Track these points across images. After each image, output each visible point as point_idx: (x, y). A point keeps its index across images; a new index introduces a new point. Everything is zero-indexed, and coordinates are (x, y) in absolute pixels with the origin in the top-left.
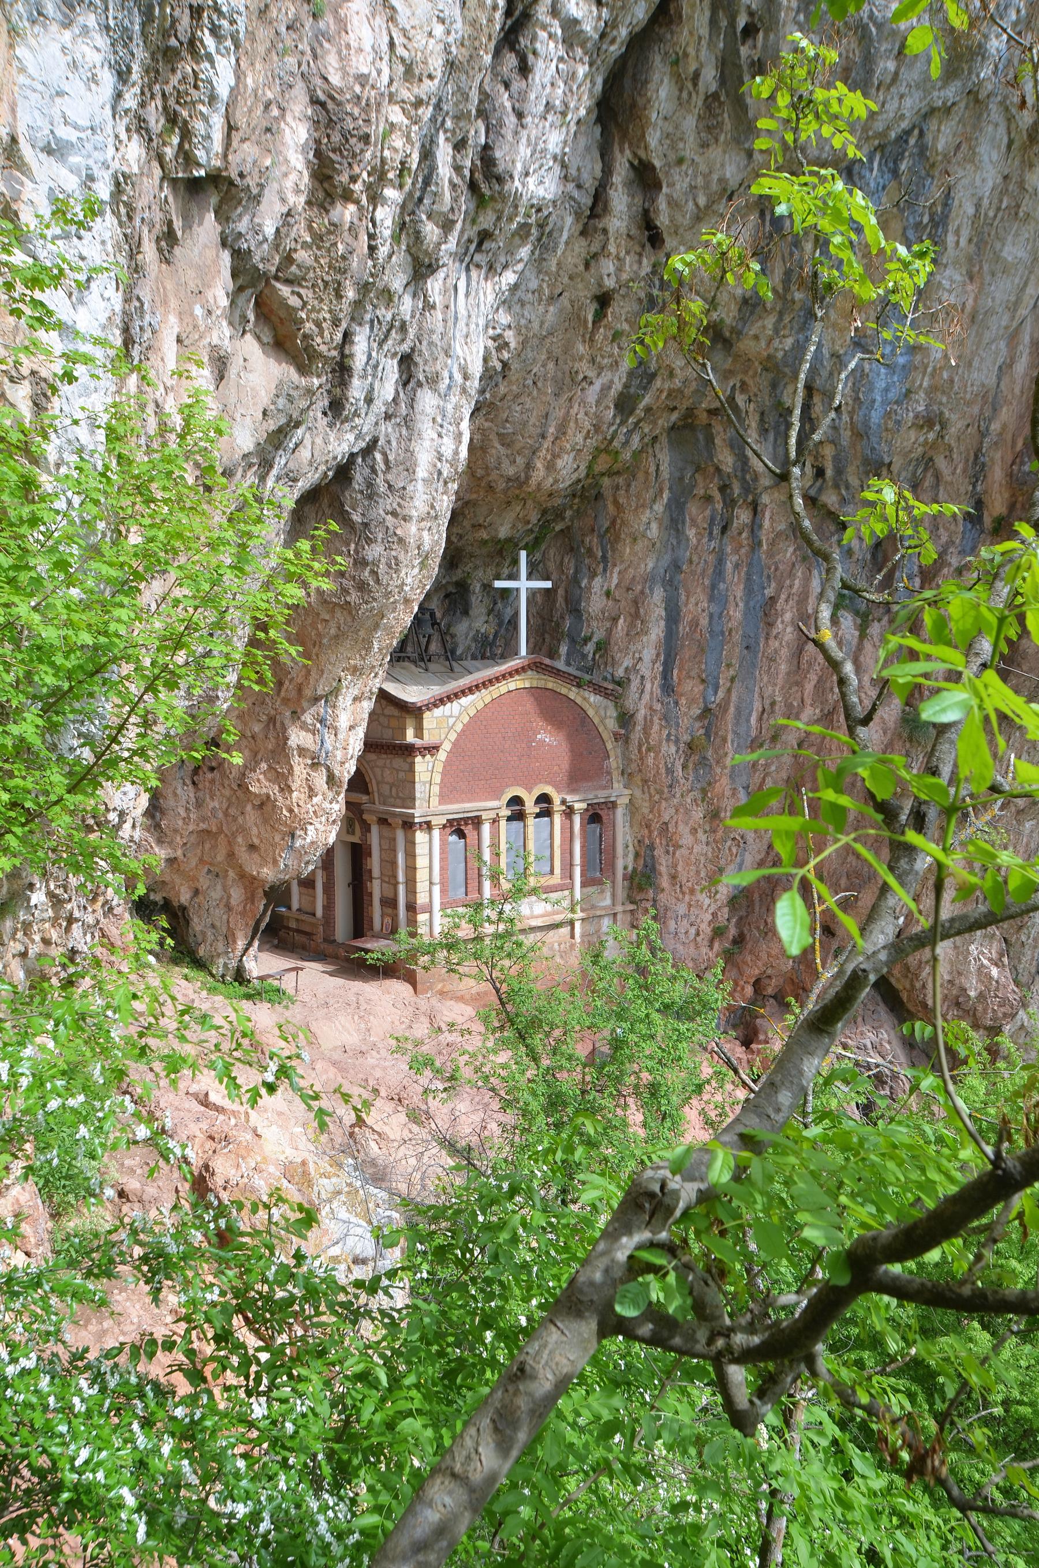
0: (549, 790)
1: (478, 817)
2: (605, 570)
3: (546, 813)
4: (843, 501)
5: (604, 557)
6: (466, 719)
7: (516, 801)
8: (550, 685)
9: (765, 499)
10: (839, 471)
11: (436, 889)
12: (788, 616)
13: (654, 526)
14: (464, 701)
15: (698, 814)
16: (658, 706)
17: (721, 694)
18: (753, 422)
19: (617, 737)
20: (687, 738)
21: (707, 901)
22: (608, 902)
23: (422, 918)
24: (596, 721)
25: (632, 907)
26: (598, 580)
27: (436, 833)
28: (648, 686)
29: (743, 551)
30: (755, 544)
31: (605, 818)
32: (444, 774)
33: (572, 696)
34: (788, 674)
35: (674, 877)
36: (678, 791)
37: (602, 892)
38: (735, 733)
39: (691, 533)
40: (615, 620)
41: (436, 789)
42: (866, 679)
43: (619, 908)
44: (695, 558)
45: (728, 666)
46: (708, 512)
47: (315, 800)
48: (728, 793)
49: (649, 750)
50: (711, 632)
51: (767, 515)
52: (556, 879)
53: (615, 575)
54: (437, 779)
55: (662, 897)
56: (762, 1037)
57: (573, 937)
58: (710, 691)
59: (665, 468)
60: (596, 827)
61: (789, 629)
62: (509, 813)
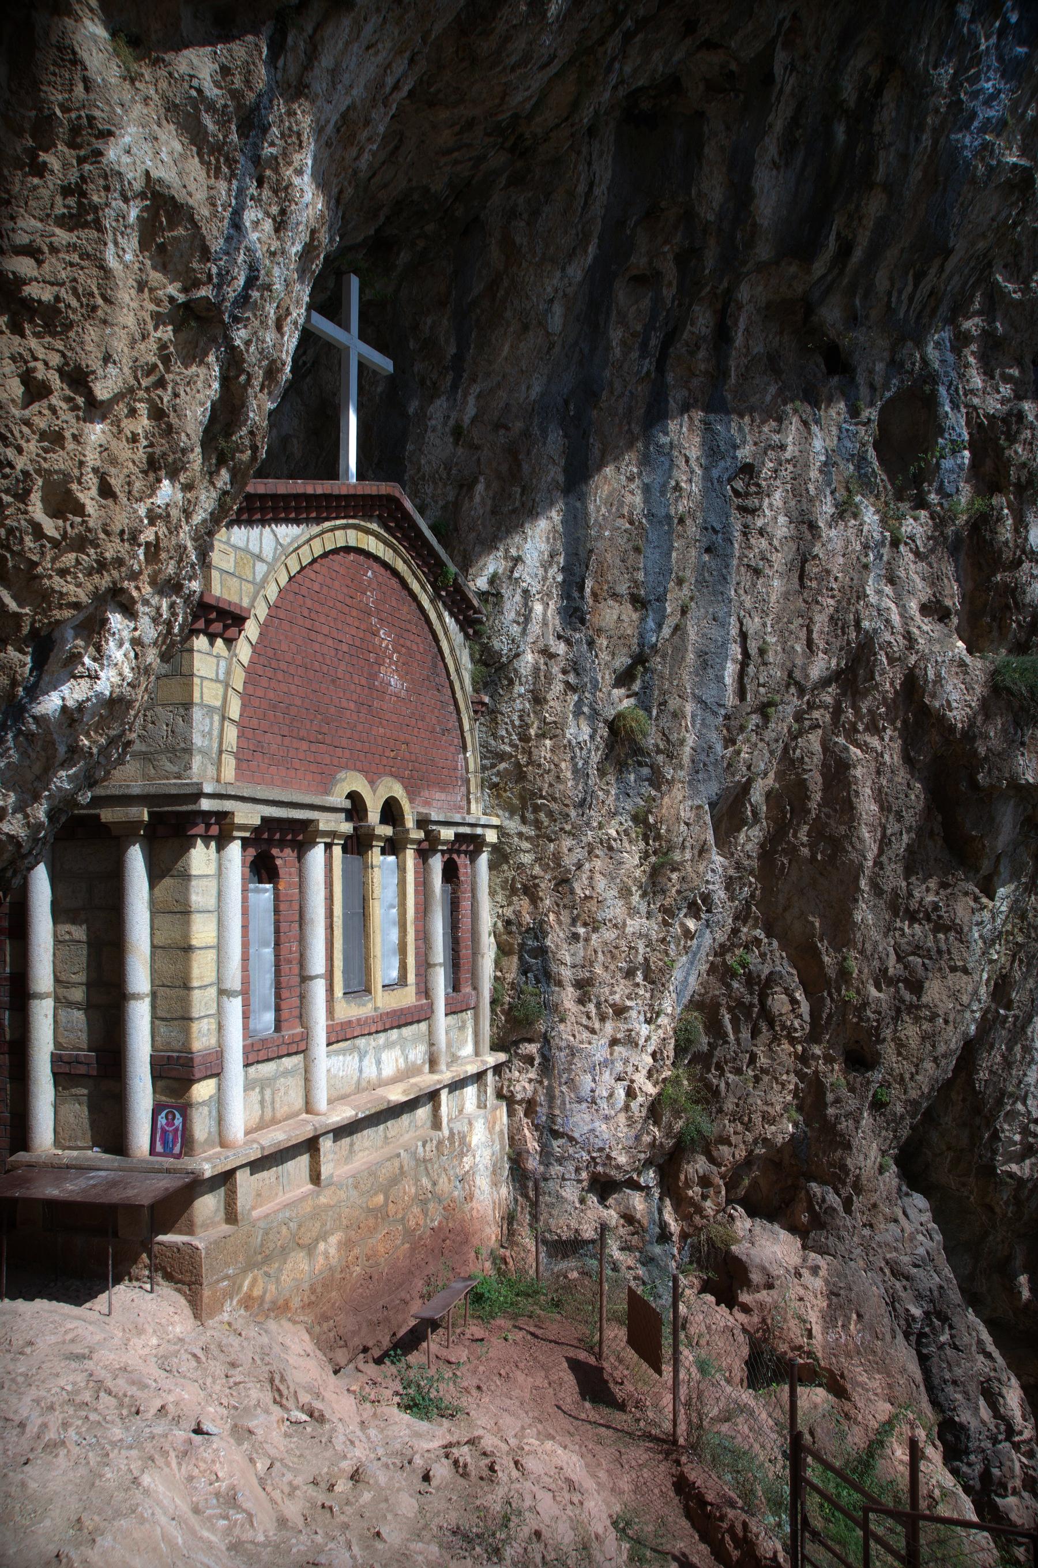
0: (398, 791)
1: (306, 824)
2: (455, 387)
3: (393, 847)
4: (853, 320)
5: (459, 358)
6: (283, 580)
7: (356, 807)
8: (400, 566)
9: (744, 293)
10: (874, 254)
11: (235, 1006)
12: (778, 495)
13: (558, 309)
14: (288, 533)
15: (631, 857)
16: (561, 648)
17: (666, 632)
18: (778, 121)
19: (479, 709)
20: (610, 713)
21: (644, 1030)
22: (468, 1049)
23: (203, 1090)
24: (452, 669)
25: (502, 1057)
26: (439, 407)
27: (235, 849)
28: (538, 608)
29: (695, 382)
30: (719, 374)
31: (462, 870)
32: (246, 698)
33: (426, 604)
34: (786, 596)
35: (584, 986)
36: (595, 816)
37: (462, 1028)
38: (700, 700)
39: (616, 335)
40: (466, 486)
41: (231, 734)
42: (913, 606)
43: (492, 1059)
44: (617, 385)
45: (680, 582)
46: (646, 303)
47: (167, 492)
48: (686, 814)
49: (541, 736)
50: (650, 515)
51: (742, 324)
52: (408, 997)
53: (471, 400)
54: (235, 710)
55: (565, 1033)
56: (756, 1277)
57: (436, 1124)
58: (651, 624)
59: (600, 191)
60: (449, 887)
61: (782, 520)
62: (347, 828)
